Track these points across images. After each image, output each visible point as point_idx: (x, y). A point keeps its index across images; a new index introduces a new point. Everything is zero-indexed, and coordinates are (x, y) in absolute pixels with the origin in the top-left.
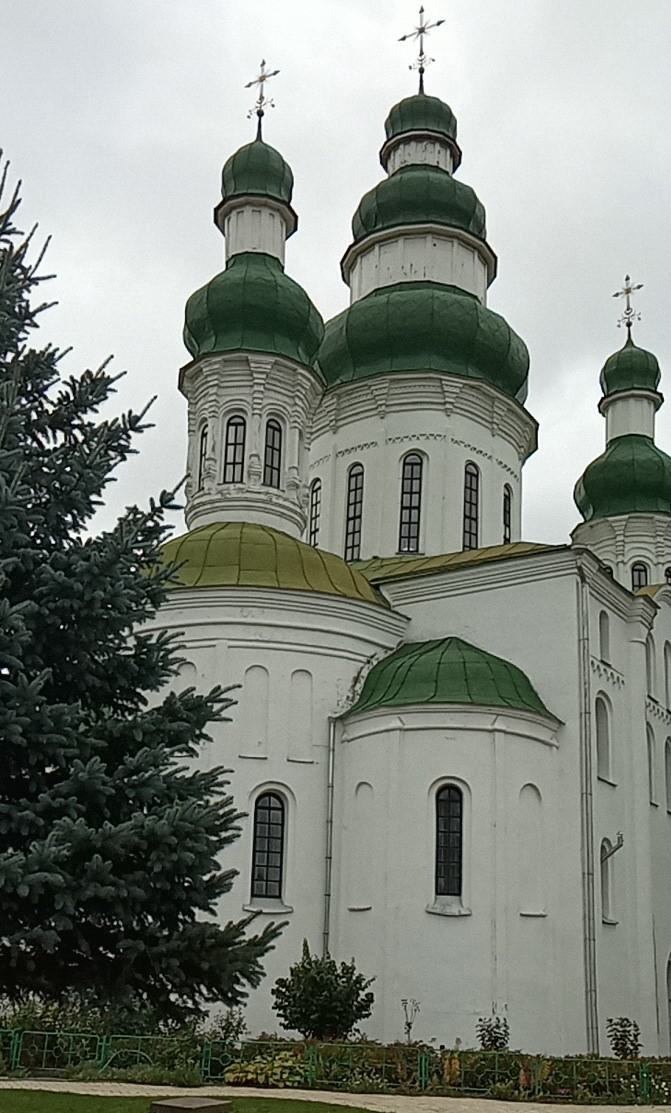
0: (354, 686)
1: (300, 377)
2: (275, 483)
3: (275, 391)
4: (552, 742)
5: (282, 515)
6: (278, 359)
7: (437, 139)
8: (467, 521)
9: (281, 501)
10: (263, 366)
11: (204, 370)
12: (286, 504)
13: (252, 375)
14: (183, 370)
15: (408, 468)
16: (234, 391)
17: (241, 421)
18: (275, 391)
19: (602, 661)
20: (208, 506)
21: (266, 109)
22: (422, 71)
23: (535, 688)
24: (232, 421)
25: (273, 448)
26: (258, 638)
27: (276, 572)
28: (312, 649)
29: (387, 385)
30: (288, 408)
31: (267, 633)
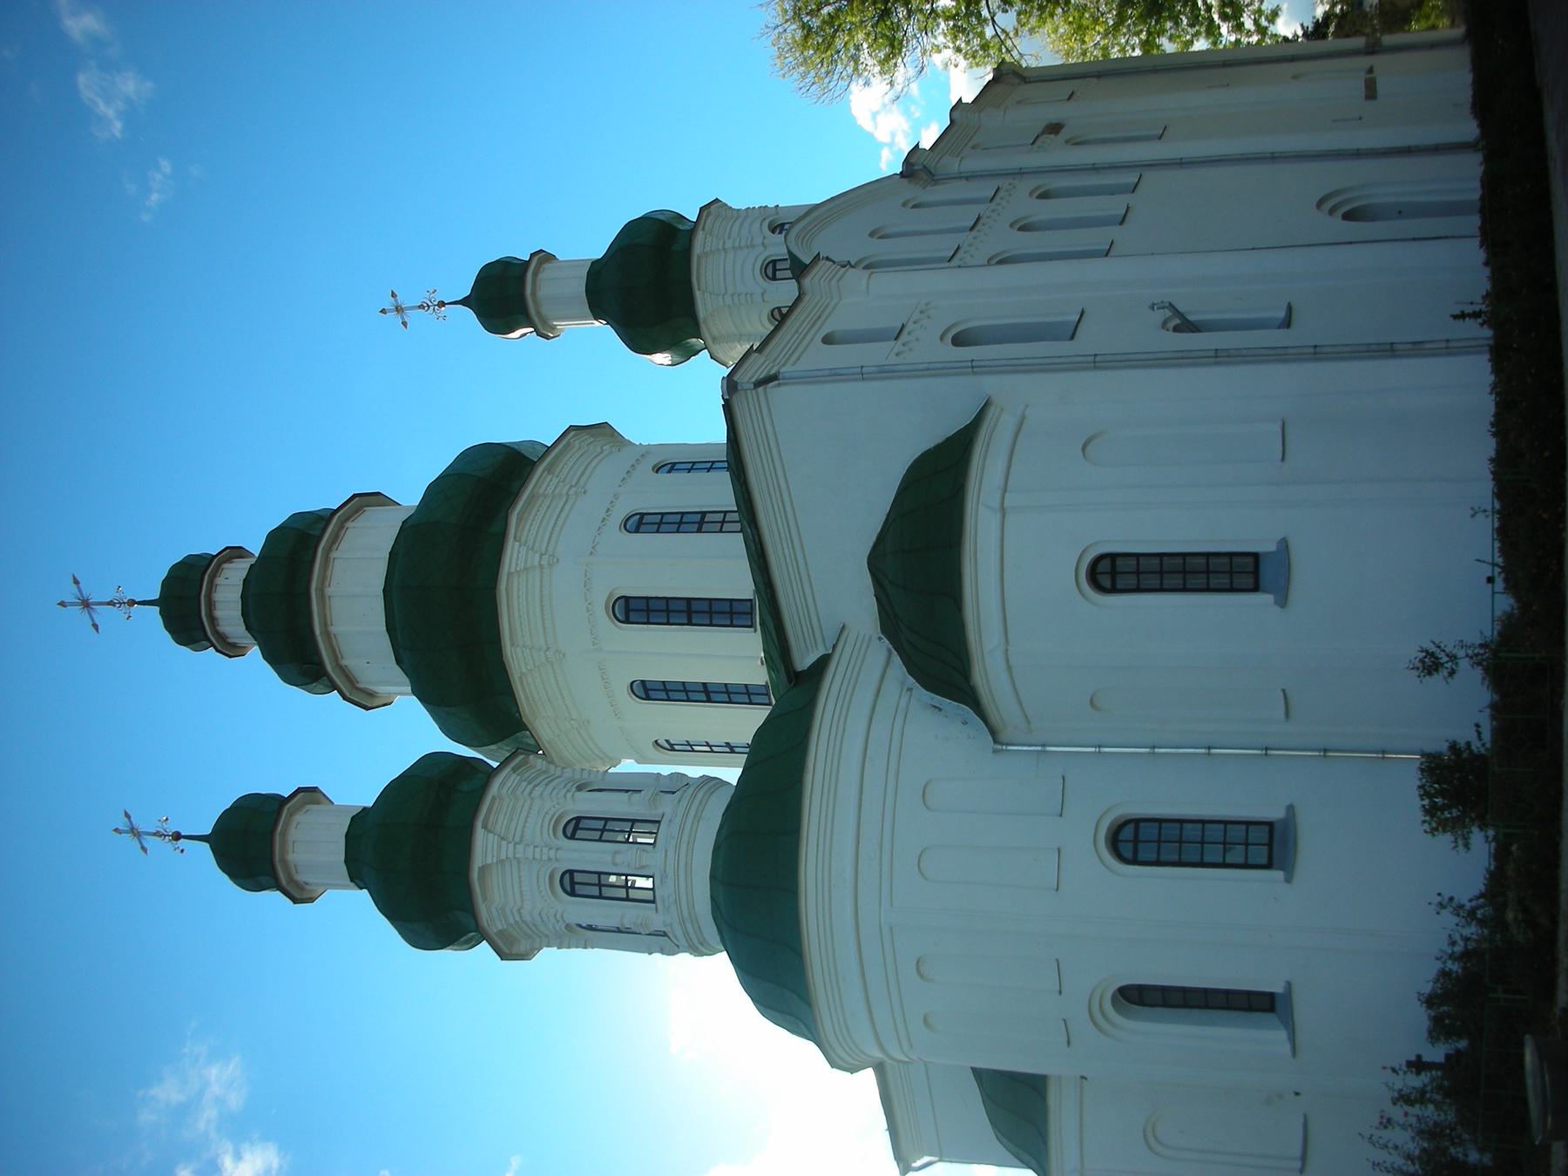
8: (705, 527)
11: (500, 928)
14: (503, 956)
15: (633, 616)
20: (689, 925)
22: (132, 603)
30: (545, 810)
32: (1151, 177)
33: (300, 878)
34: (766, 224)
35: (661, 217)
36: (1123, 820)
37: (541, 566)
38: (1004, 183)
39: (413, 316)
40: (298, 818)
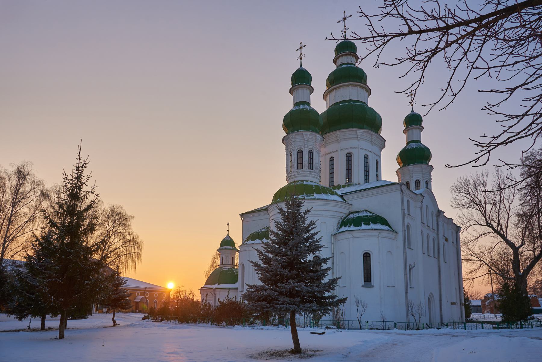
0: (337, 226)
2: (312, 168)
15: (347, 157)
17: (301, 151)
19: (408, 214)
23: (389, 223)
25: (311, 158)
32: (436, 260)
34: (428, 180)
37: (358, 138)
38: (436, 232)
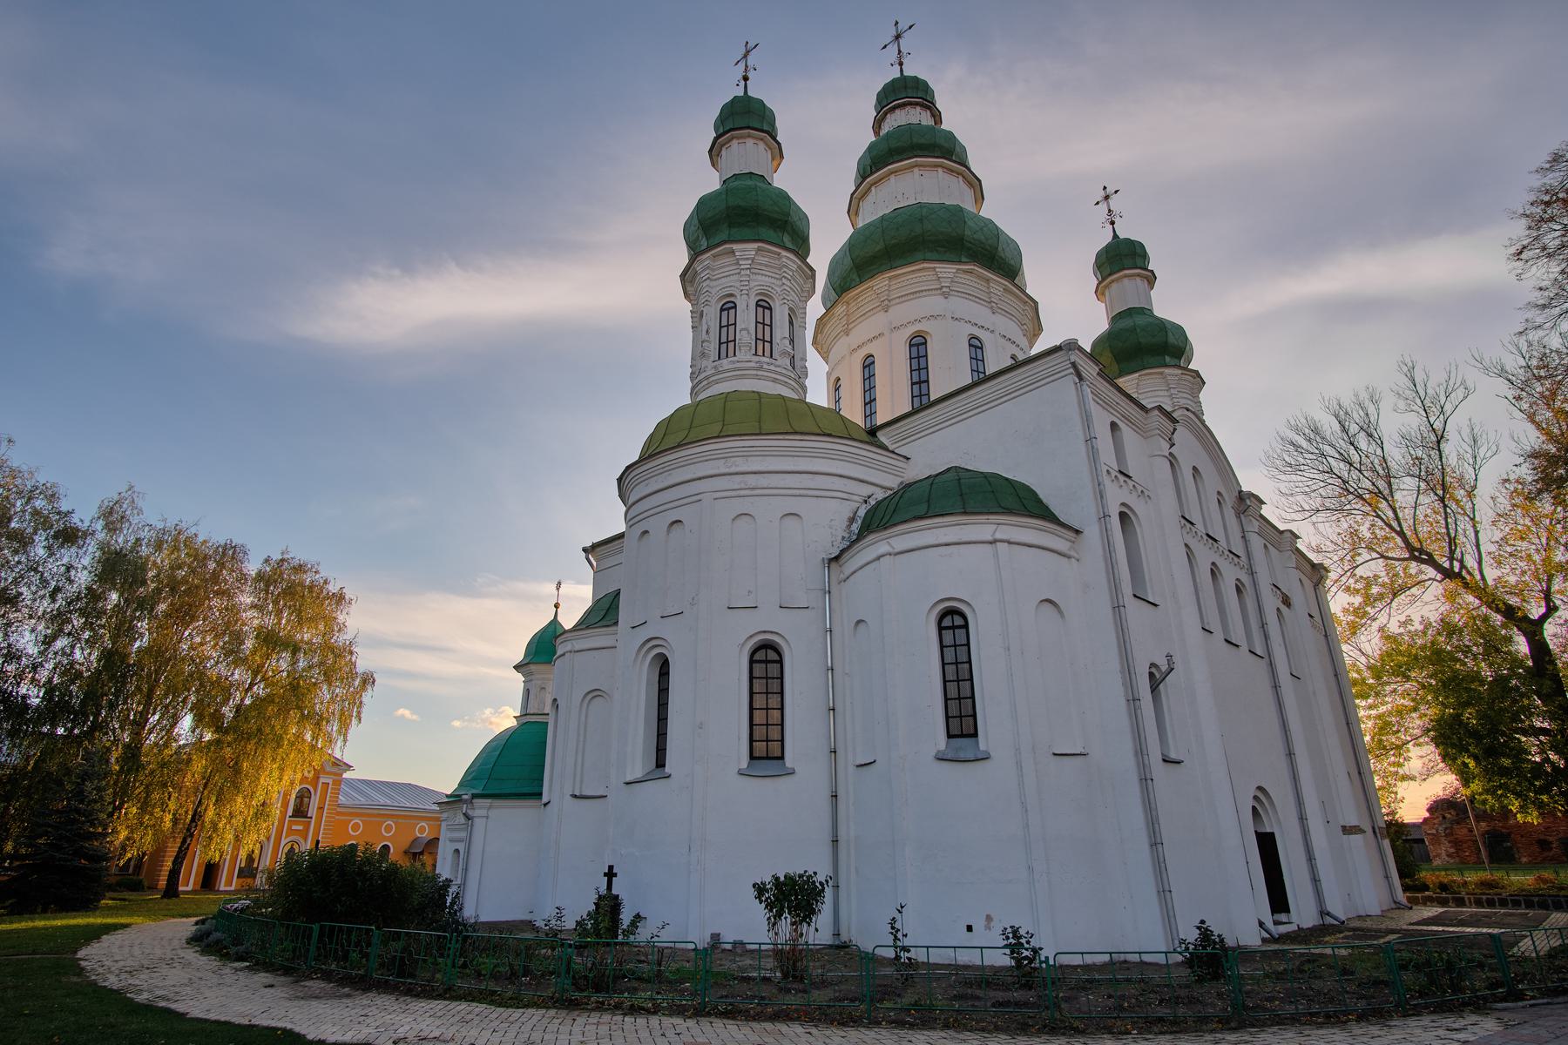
0: (849, 526)
1: (784, 260)
3: (762, 275)
4: (1068, 553)
5: (775, 380)
6: (760, 244)
7: (917, 104)
9: (772, 368)
10: (746, 253)
12: (778, 369)
13: (738, 264)
15: (914, 349)
16: (723, 280)
17: (733, 305)
18: (762, 275)
19: (1121, 472)
20: (705, 382)
21: (751, 75)
22: (901, 64)
23: (1045, 501)
24: (725, 307)
26: (743, 486)
27: (760, 422)
28: (797, 492)
29: (887, 282)
30: (775, 288)
31: (752, 480)
32: (1263, 663)
33: (724, 152)
35: (1188, 348)
36: (782, 652)
39: (1103, 207)
40: (762, 145)
